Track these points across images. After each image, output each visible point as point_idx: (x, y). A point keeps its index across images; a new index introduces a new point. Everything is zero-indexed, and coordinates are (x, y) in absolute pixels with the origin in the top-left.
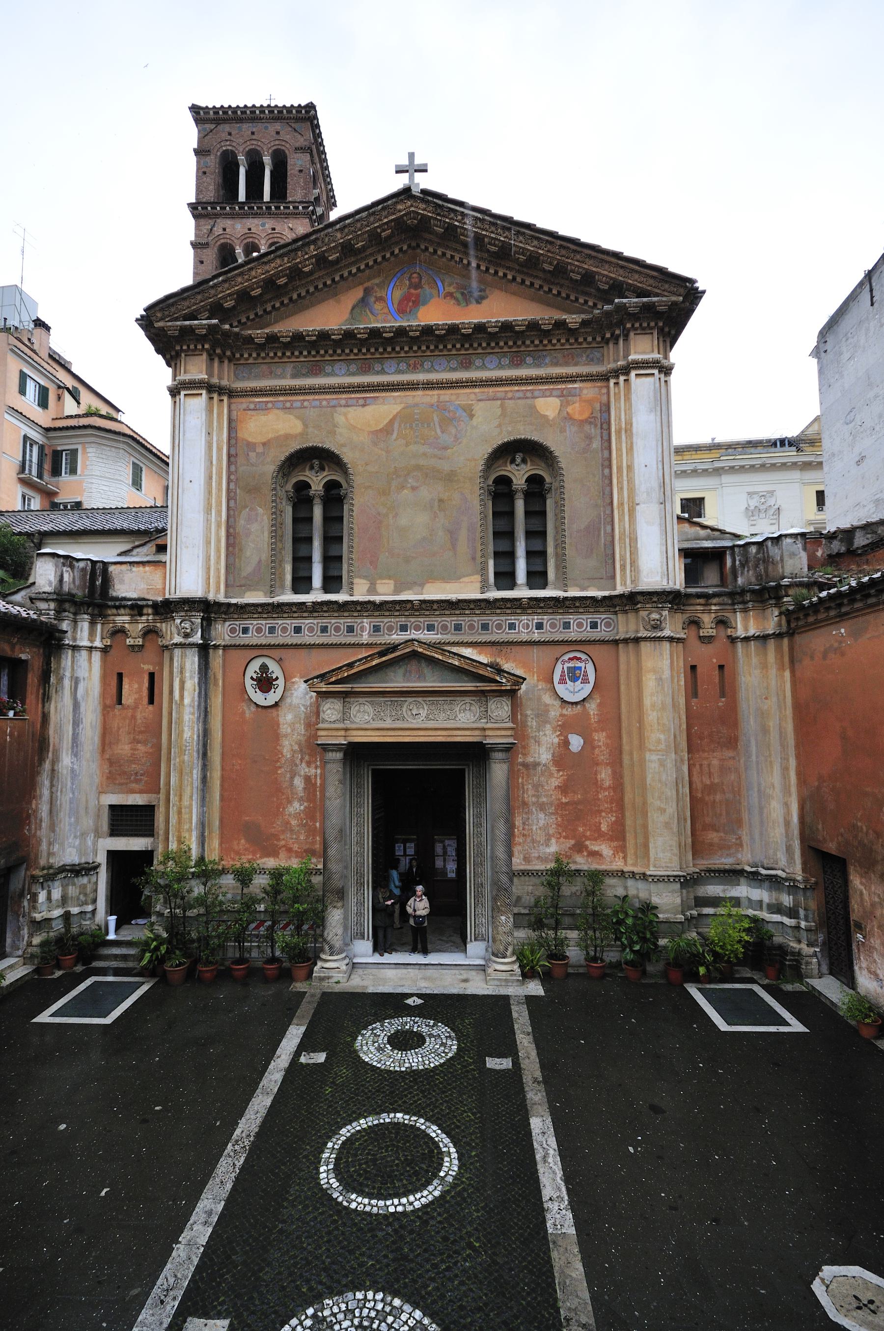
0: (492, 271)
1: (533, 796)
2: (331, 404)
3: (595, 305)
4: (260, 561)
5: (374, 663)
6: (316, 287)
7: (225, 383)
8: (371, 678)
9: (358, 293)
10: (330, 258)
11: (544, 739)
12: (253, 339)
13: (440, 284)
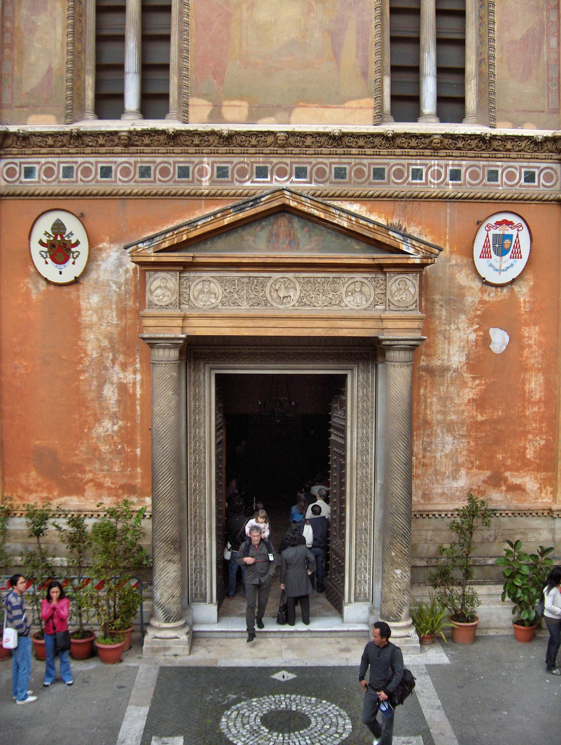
1: (438, 412)
4: (50, 70)
5: (227, 221)
8: (220, 243)
11: (456, 335)
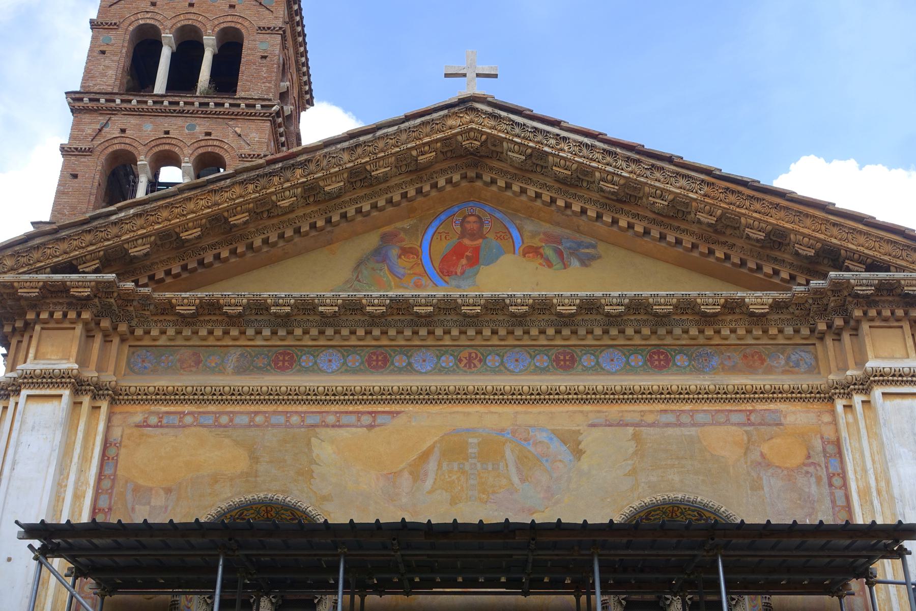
0: (607, 219)
2: (310, 421)
3: (793, 278)
6: (297, 231)
7: (108, 377)
9: (371, 241)
10: (327, 189)
12: (173, 307)
13: (515, 233)
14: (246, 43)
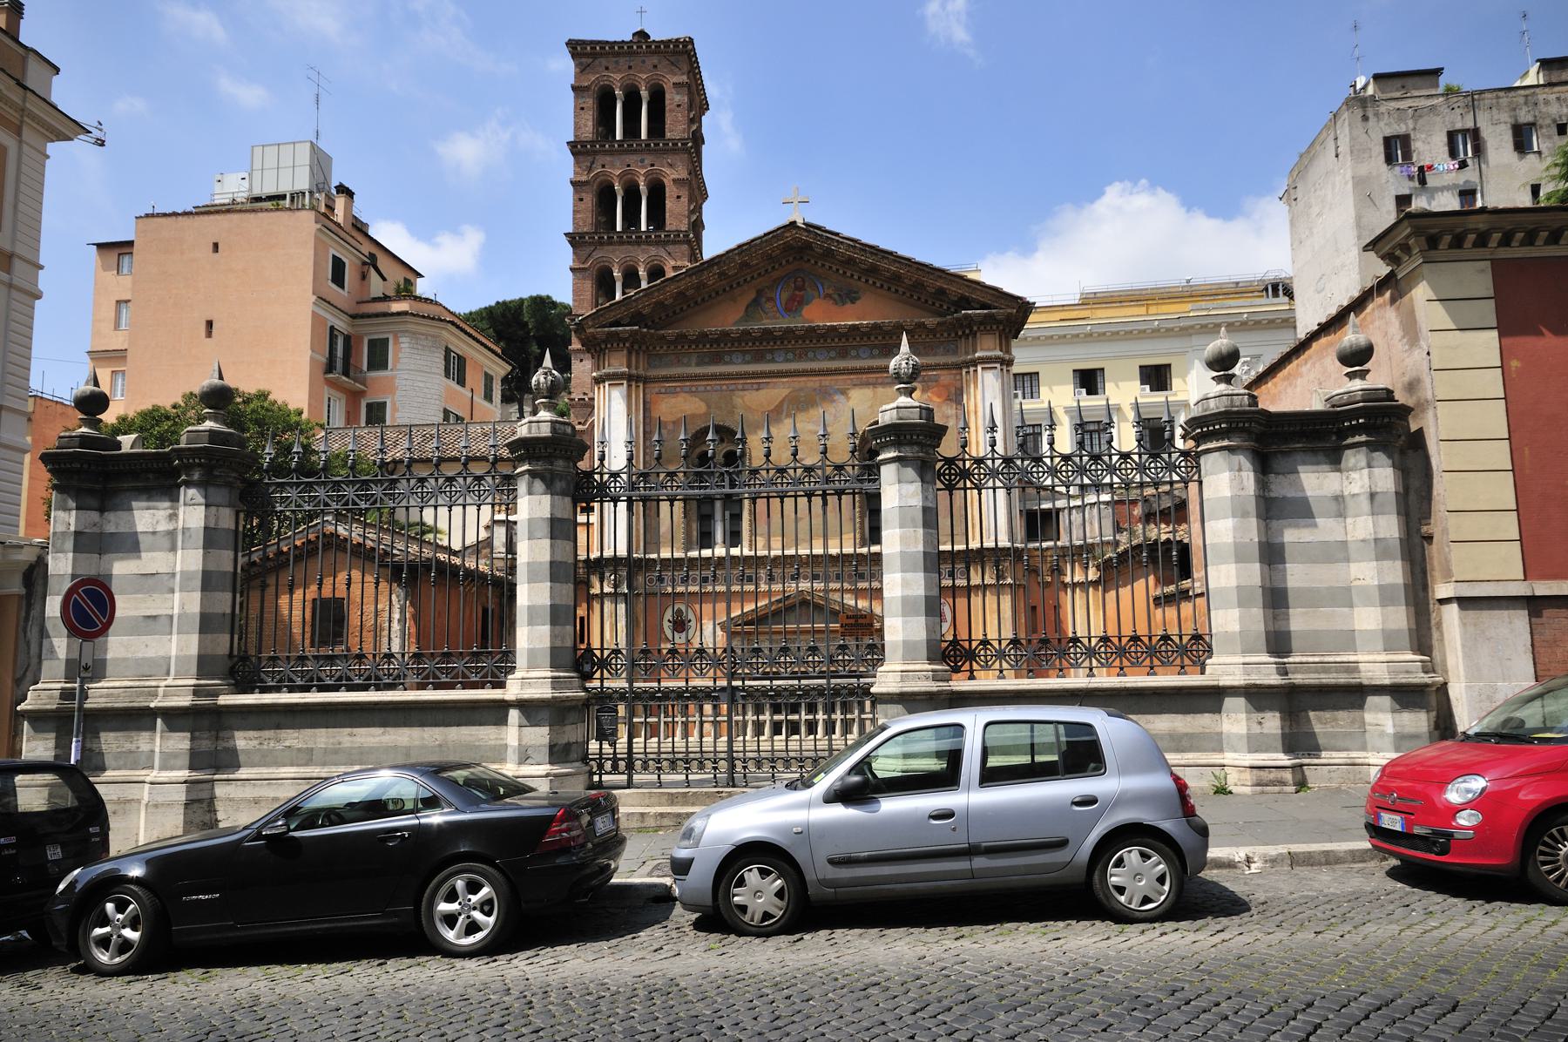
7: (641, 372)
9: (753, 295)
13: (820, 288)
14: (668, 96)
